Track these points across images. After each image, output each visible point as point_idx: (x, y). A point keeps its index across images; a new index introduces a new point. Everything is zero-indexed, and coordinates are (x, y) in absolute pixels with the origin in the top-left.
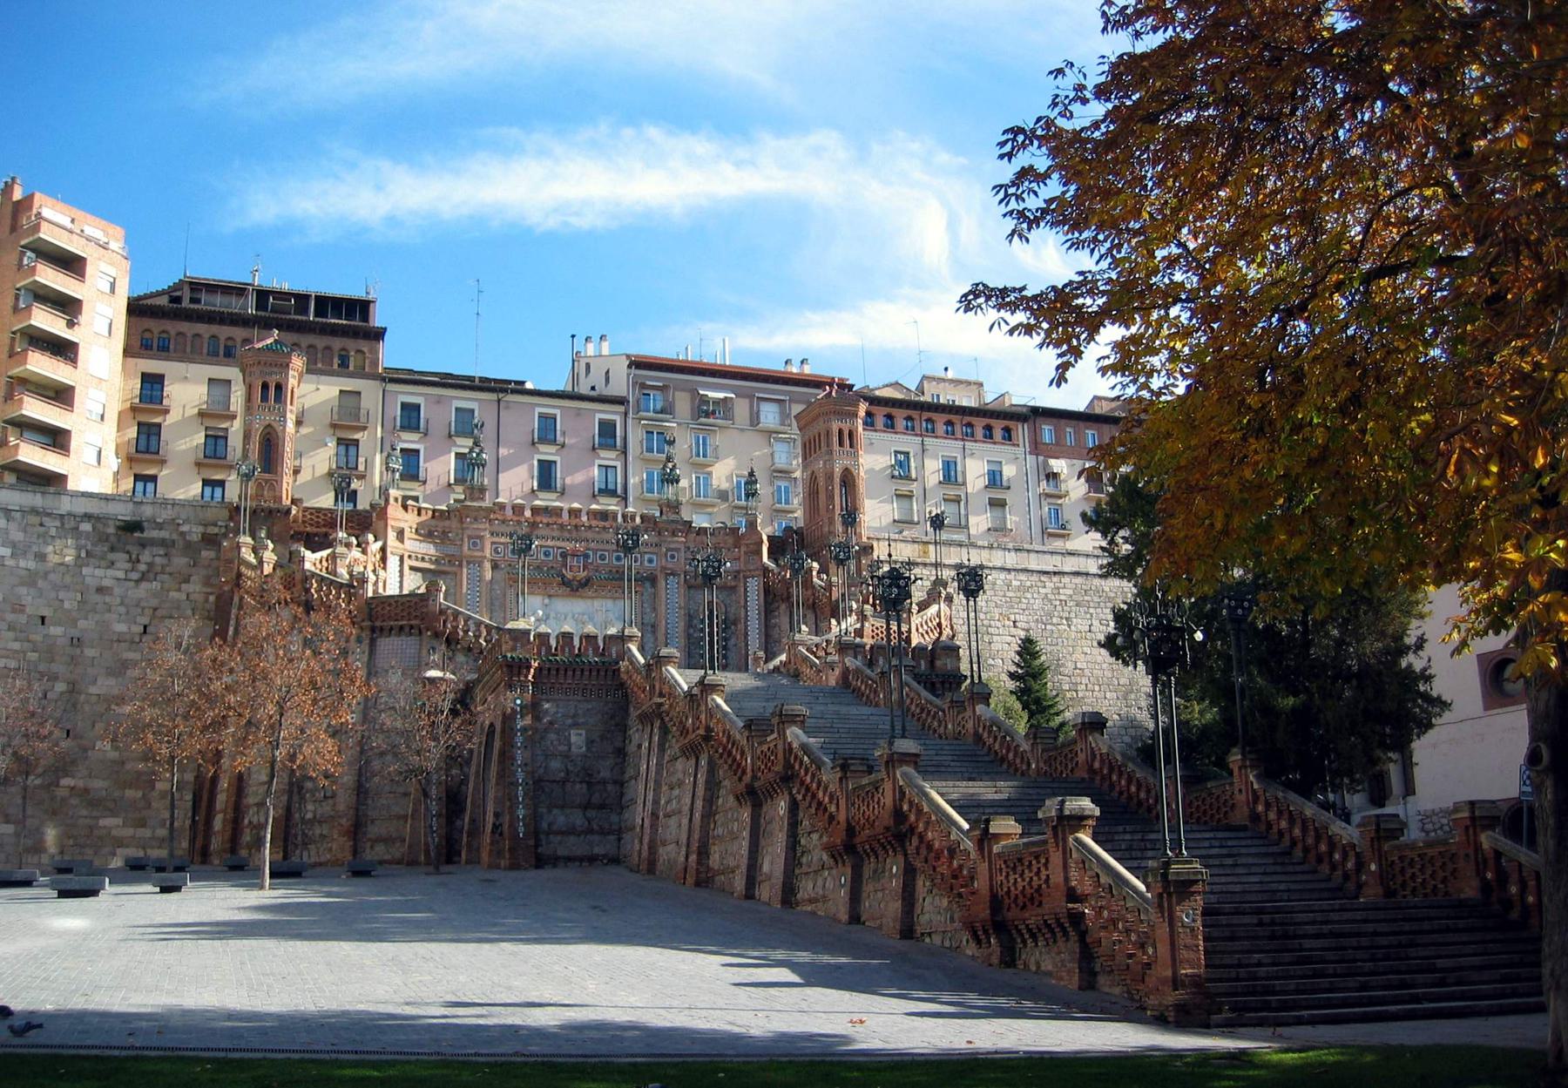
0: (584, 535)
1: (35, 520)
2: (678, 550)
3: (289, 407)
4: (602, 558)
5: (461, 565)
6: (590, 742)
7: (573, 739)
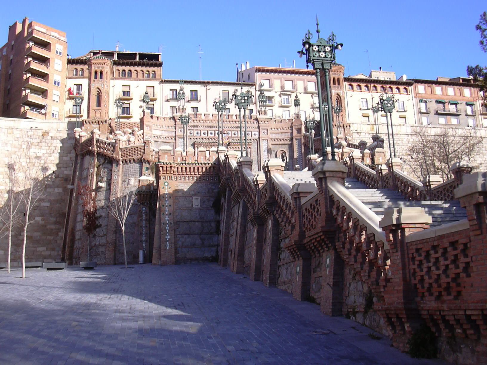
1: (10, 131)
3: (105, 80)
6: (202, 202)
7: (194, 200)
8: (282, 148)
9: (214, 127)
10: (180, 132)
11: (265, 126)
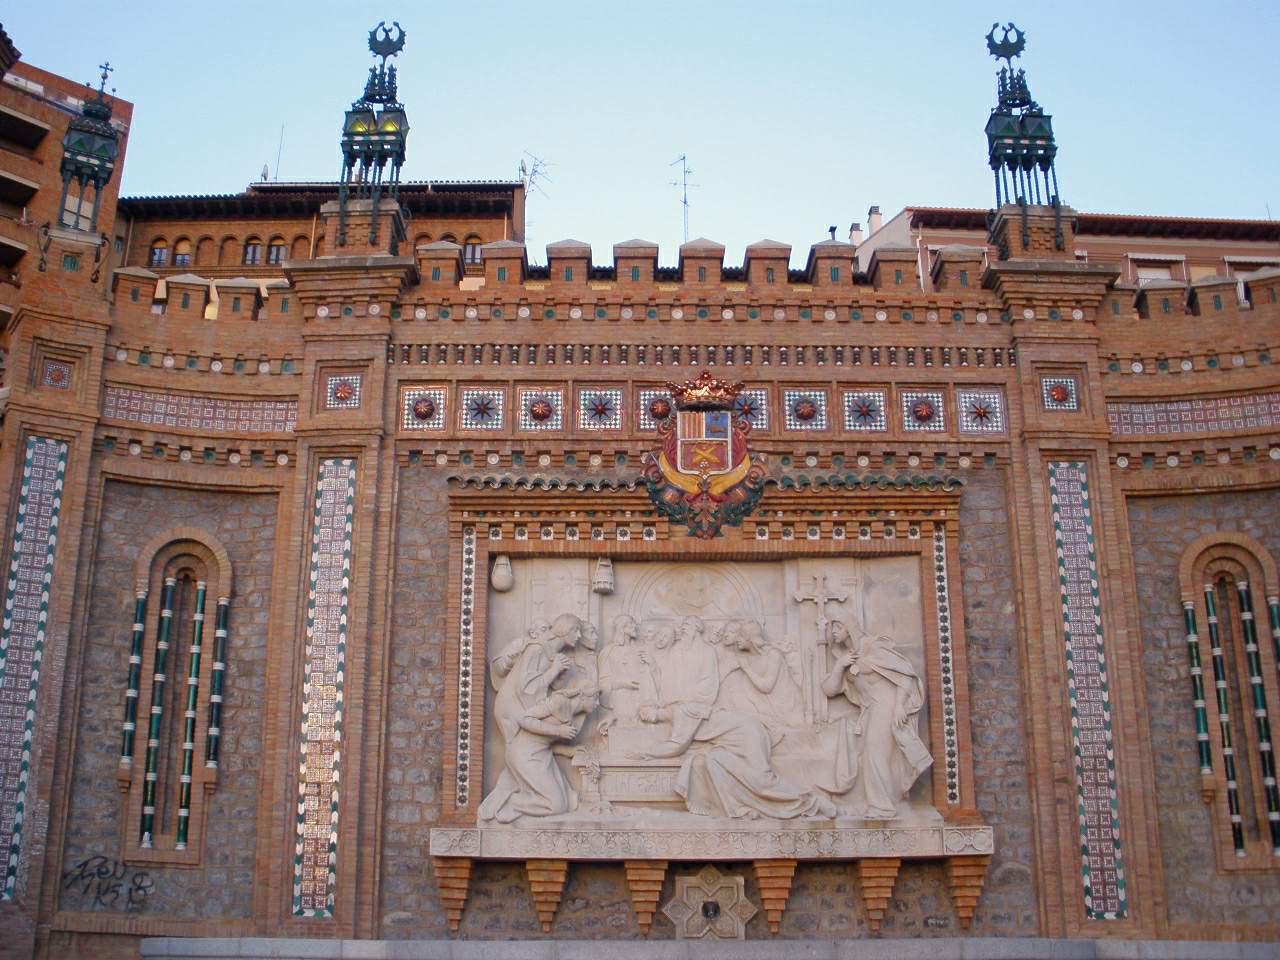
0: (734, 335)
2: (1075, 368)
4: (806, 414)
5: (292, 465)
8: (1219, 526)
10: (331, 403)
11: (1057, 341)
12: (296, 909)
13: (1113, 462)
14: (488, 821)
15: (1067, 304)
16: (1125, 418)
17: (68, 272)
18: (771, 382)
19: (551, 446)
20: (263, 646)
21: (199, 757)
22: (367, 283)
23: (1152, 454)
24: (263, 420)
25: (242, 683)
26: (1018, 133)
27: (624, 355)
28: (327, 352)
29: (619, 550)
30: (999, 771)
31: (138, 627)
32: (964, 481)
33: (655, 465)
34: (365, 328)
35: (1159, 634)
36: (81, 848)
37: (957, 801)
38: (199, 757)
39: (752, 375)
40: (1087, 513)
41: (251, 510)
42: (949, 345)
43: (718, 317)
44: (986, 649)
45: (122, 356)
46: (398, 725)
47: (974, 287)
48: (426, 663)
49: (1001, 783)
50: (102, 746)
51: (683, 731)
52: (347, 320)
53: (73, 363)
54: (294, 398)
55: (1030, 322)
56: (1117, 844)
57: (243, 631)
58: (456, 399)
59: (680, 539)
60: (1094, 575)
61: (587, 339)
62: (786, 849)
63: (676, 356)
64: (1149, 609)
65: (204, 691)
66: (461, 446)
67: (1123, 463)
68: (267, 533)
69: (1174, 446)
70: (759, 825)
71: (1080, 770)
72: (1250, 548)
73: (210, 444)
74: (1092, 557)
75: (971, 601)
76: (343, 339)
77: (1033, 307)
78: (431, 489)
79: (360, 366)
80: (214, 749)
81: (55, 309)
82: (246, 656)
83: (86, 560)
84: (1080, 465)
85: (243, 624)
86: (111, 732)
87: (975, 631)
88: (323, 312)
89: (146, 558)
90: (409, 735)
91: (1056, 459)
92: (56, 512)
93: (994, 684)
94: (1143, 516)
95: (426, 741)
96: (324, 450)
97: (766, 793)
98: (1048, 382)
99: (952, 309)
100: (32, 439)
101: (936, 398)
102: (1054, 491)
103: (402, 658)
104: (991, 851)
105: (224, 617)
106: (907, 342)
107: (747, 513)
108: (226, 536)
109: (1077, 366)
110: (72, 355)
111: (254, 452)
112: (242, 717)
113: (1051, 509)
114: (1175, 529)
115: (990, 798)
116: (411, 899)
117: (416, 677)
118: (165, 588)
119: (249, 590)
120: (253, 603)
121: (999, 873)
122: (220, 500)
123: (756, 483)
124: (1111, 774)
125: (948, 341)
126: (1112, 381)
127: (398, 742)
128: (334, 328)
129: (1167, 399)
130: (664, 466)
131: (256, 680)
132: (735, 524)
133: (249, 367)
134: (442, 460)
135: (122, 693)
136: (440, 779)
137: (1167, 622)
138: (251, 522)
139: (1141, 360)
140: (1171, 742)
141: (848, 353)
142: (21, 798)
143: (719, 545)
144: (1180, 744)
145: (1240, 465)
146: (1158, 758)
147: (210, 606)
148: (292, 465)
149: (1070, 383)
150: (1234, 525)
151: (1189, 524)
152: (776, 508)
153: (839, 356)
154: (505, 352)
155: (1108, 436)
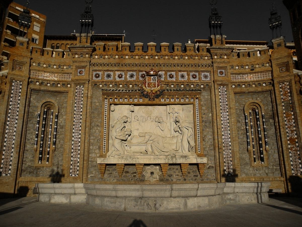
0: (158, 62)
2: (225, 68)
9: (136, 65)
10: (79, 74)
11: (221, 63)
12: (71, 175)
13: (232, 86)
14: (109, 156)
15: (224, 55)
16: (234, 78)
17: (21, 46)
18: (165, 71)
19: (122, 83)
20: (65, 123)
21: (51, 145)
22: (85, 50)
23: (240, 85)
24: (65, 78)
25: (61, 130)
26: (215, 21)
27: (136, 65)
28: (77, 64)
29: (135, 103)
30: (208, 146)
31: (38, 119)
32: (202, 90)
33: (142, 87)
34: (85, 60)
35: (240, 120)
36: (26, 164)
37: (200, 152)
38: (51, 145)
39: (161, 69)
40: (226, 96)
41: (63, 96)
42: (200, 63)
43: (155, 58)
44: (206, 123)
45: (34, 64)
46: (92, 138)
47: (205, 52)
48: (98, 125)
49: (209, 149)
50: (30, 143)
51: (147, 137)
52: (82, 58)
53: (23, 65)
54: (71, 73)
55: (216, 59)
56: (231, 161)
57: (61, 120)
58: (104, 74)
59: (147, 101)
60: (227, 108)
61: (129, 62)
62: (167, 161)
63: (146, 66)
64: (238, 115)
65: (53, 132)
66: (105, 83)
67: (234, 86)
68: (66, 100)
69: (244, 83)
70: (161, 157)
71: (224, 147)
72: (259, 103)
73: (54, 82)
74: (227, 105)
75: (203, 113)
76: (81, 62)
77: (217, 56)
78: (99, 91)
79: (84, 67)
80: (55, 143)
81: (19, 54)
82: (61, 124)
83: (27, 106)
84: (225, 87)
85: (61, 118)
86: (33, 140)
87: (204, 119)
88: (77, 56)
89: (40, 105)
90: (94, 140)
91: (220, 86)
92: (20, 96)
93: (207, 129)
94: (237, 97)
95: (97, 141)
96: (77, 84)
97: (162, 150)
98: (219, 71)
99: (200, 56)
100: (14, 81)
101: (197, 74)
102: (220, 92)
103: (93, 124)
104: (206, 162)
105: (57, 117)
106: (191, 63)
107: (160, 96)
108: (57, 101)
109: (225, 67)
110: (22, 64)
111: (63, 84)
112: (61, 137)
113: (219, 95)
114: (244, 100)
115: (206, 152)
116: (94, 172)
117: (96, 128)
118: (44, 111)
119: (62, 111)
120: (63, 114)
121: (208, 166)
122: (56, 94)
123: (162, 90)
124: (230, 147)
125: (199, 63)
126: (232, 70)
127: (92, 141)
128: (79, 60)
129: (243, 74)
130: (144, 87)
131: (63, 129)
132: (157, 98)
133: (62, 67)
134: (101, 86)
135: (35, 133)
136: (100, 148)
137: (242, 118)
138: (63, 98)
139: (238, 66)
140: (242, 141)
141: (180, 65)
142: (12, 154)
143: (154, 102)
144: (244, 142)
145: (257, 87)
146: (239, 144)
147: (54, 114)
148: (71, 87)
149: (223, 71)
150: (256, 99)
151: (246, 99)
152: (165, 95)
153: (178, 66)
154: (113, 65)
155: (231, 81)
